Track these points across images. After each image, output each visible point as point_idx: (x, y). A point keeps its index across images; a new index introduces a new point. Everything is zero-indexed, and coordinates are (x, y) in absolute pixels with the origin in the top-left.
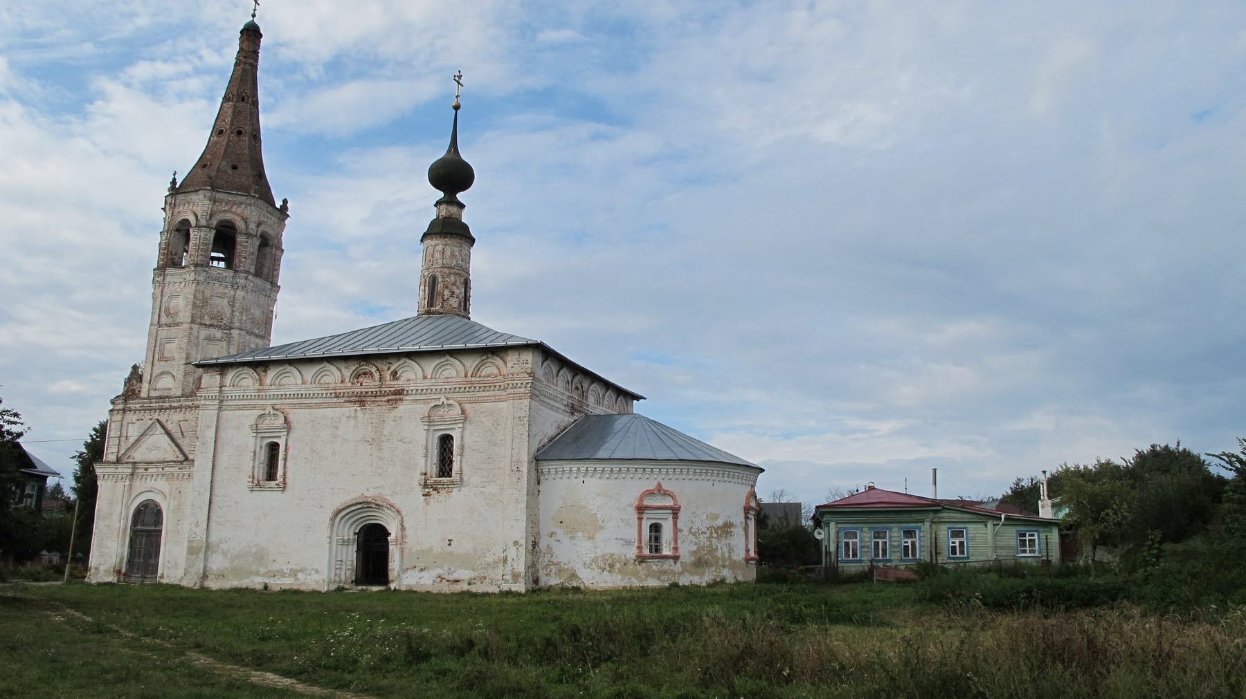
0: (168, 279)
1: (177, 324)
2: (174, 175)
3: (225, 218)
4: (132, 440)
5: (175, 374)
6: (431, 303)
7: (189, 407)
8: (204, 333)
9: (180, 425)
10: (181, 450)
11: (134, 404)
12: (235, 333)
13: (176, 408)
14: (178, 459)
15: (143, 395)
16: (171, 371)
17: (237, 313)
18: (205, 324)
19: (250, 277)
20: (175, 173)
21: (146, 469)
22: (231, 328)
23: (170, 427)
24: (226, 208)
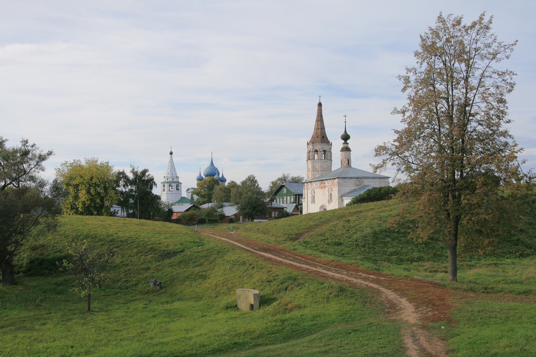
6: (342, 165)
8: (314, 173)
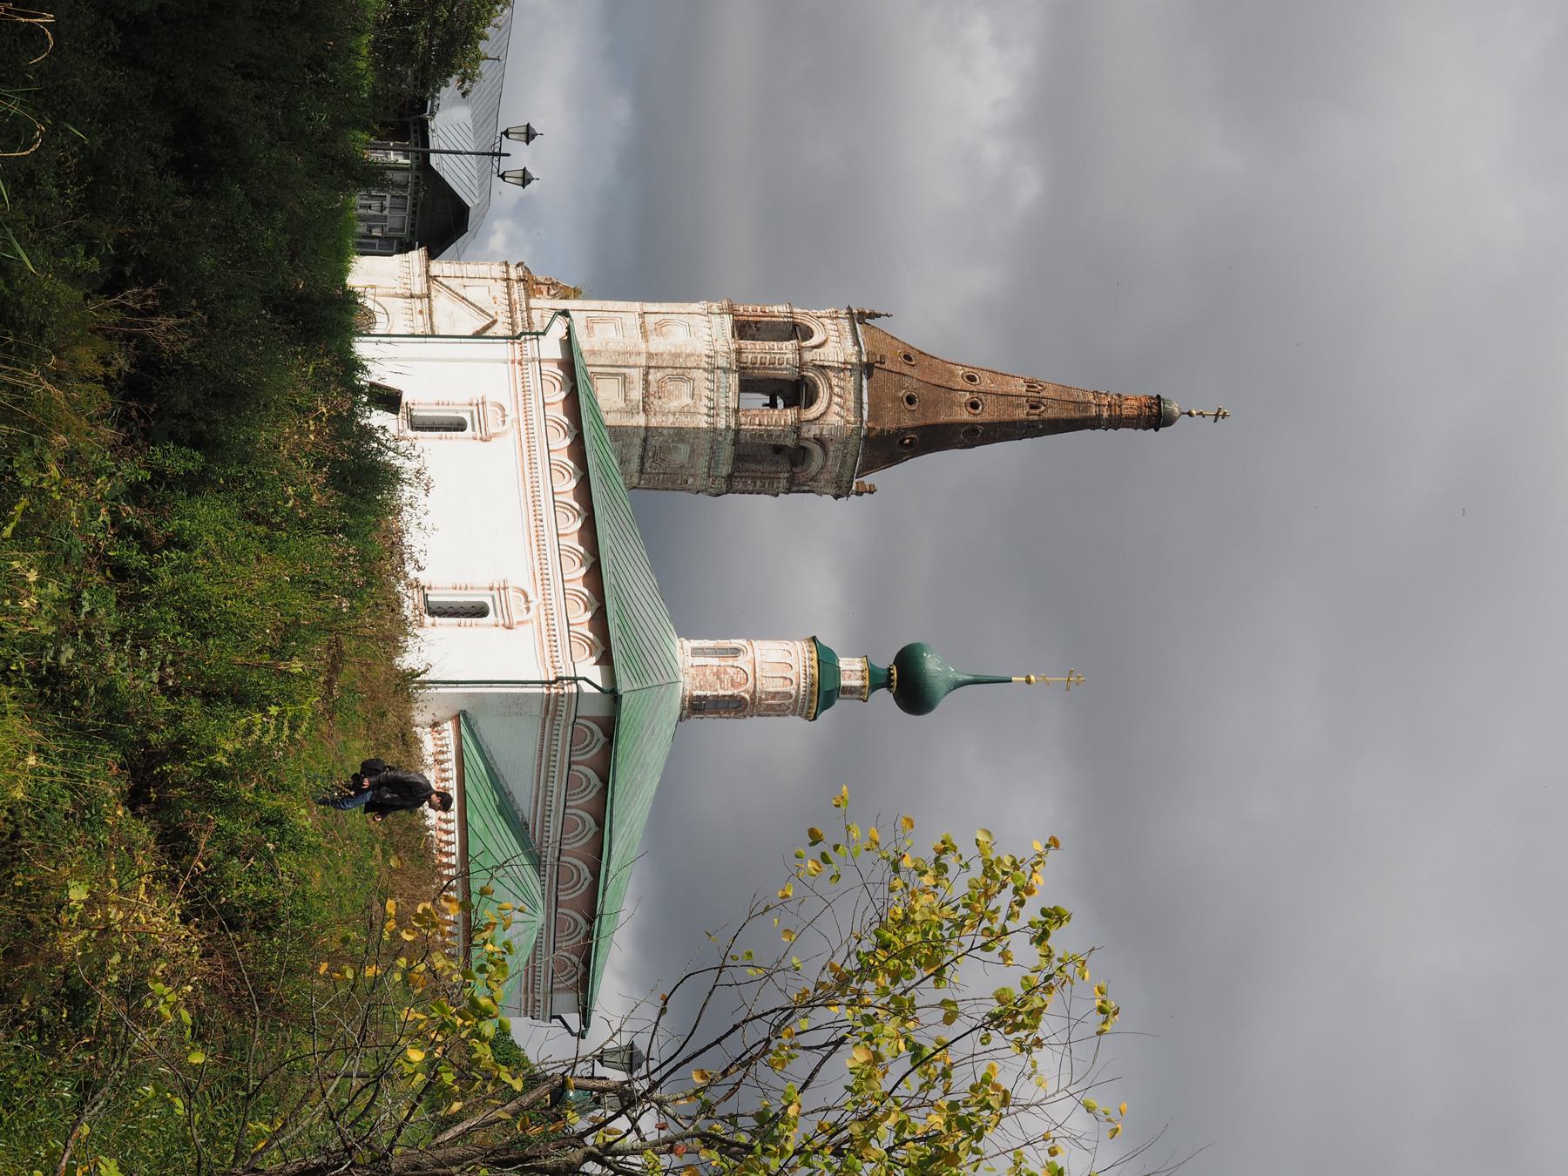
0: (716, 319)
1: (645, 335)
2: (887, 315)
3: (821, 389)
4: (462, 292)
11: (518, 291)
15: (533, 303)
21: (421, 312)
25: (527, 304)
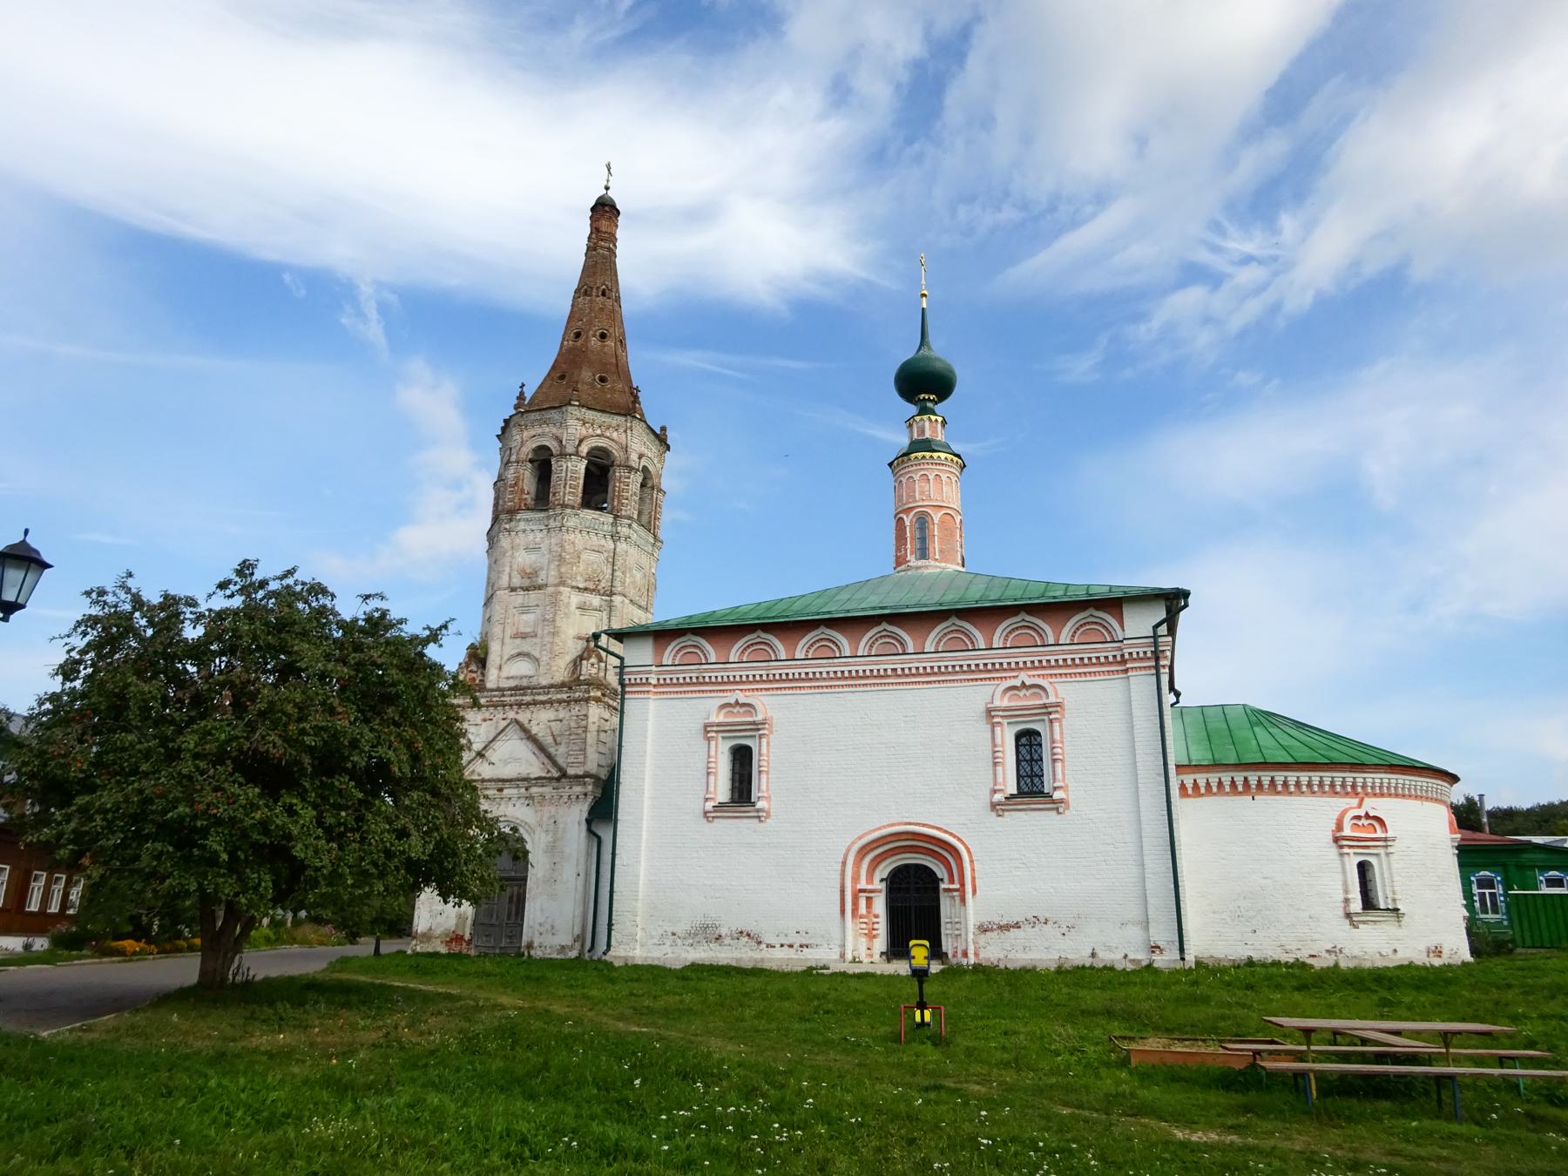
1: (540, 587)
3: (600, 445)
5: (537, 656)
7: (564, 701)
8: (576, 599)
9: (550, 728)
10: (555, 763)
12: (617, 599)
13: (543, 703)
14: (549, 775)
15: (489, 685)
16: (533, 653)
17: (618, 573)
18: (578, 588)
19: (635, 525)
20: (523, 385)
21: (500, 790)
22: (612, 594)
23: (535, 730)
24: (599, 432)
25: (492, 690)
